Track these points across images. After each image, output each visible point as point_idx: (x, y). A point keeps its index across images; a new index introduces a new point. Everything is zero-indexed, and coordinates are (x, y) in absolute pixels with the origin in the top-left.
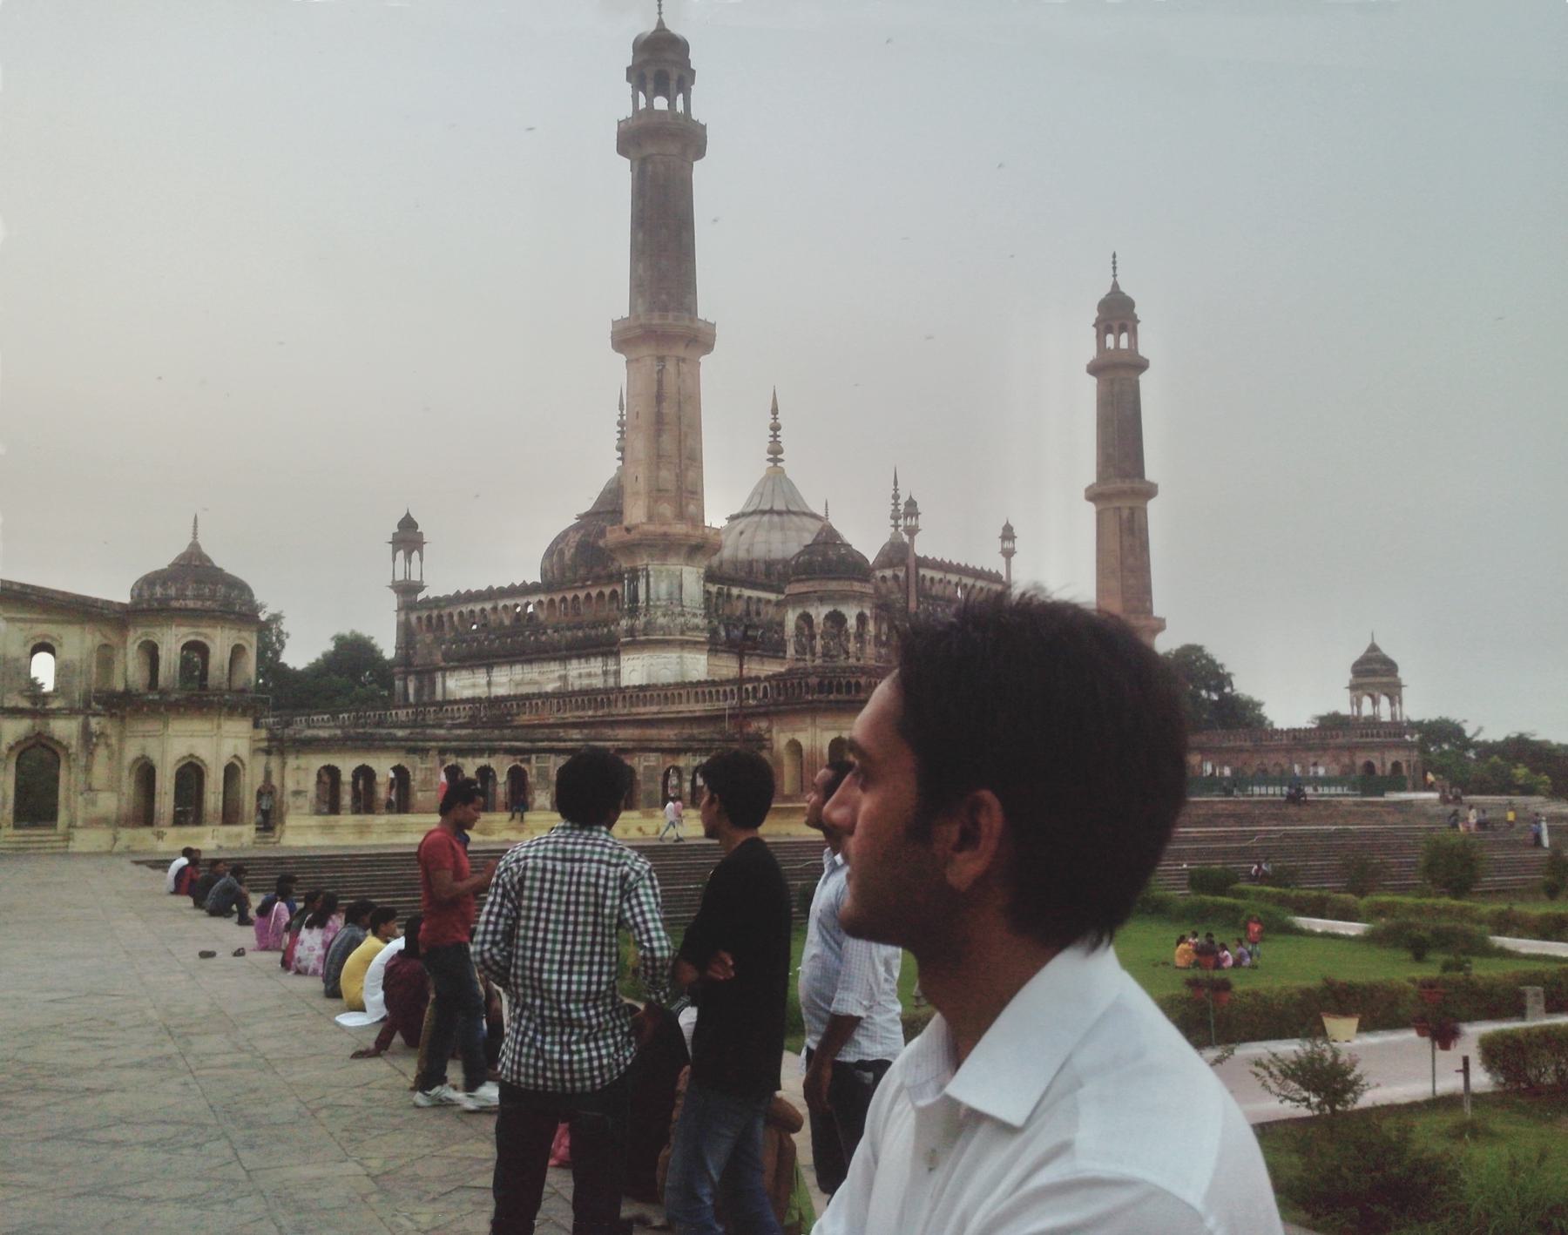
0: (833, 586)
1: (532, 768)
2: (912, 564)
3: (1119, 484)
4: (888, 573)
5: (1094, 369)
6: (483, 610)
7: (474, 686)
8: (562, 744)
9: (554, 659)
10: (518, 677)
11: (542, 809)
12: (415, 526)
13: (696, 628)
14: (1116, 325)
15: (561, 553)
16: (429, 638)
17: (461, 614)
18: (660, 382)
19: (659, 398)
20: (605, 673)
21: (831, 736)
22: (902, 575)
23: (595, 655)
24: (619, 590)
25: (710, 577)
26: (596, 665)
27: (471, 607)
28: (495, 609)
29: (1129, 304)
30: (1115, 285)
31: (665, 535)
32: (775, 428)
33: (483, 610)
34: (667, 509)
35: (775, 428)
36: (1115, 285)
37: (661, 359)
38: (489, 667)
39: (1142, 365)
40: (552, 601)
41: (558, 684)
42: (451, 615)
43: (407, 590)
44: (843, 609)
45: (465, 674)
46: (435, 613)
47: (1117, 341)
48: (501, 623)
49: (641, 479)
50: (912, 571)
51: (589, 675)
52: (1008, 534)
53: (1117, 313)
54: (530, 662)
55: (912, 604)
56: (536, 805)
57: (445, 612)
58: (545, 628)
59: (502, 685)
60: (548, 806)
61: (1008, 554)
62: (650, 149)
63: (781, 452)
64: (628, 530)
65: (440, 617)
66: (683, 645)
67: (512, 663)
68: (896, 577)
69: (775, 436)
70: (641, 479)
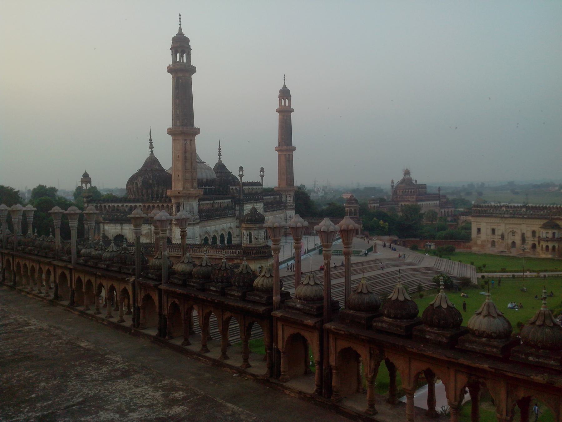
0: (258, 225)
2: (241, 185)
3: (285, 148)
4: (234, 188)
5: (278, 111)
6: (118, 206)
7: (116, 229)
12: (88, 175)
13: (197, 219)
15: (136, 184)
17: (109, 206)
19: (185, 152)
21: (259, 266)
22: (238, 189)
24: (170, 205)
27: (113, 204)
28: (123, 206)
29: (289, 91)
30: (285, 85)
31: (189, 194)
33: (118, 206)
34: (188, 185)
36: (285, 85)
37: (186, 140)
38: (122, 224)
39: (293, 111)
40: (144, 206)
42: (105, 206)
45: (112, 225)
46: (99, 205)
47: (285, 102)
48: (125, 210)
49: (180, 176)
50: (241, 189)
52: (262, 170)
53: (285, 94)
55: (242, 198)
57: (103, 205)
59: (126, 229)
61: (262, 176)
62: (180, 75)
64: (179, 193)
65: (101, 206)
66: (194, 224)
68: (236, 189)
70: (180, 176)
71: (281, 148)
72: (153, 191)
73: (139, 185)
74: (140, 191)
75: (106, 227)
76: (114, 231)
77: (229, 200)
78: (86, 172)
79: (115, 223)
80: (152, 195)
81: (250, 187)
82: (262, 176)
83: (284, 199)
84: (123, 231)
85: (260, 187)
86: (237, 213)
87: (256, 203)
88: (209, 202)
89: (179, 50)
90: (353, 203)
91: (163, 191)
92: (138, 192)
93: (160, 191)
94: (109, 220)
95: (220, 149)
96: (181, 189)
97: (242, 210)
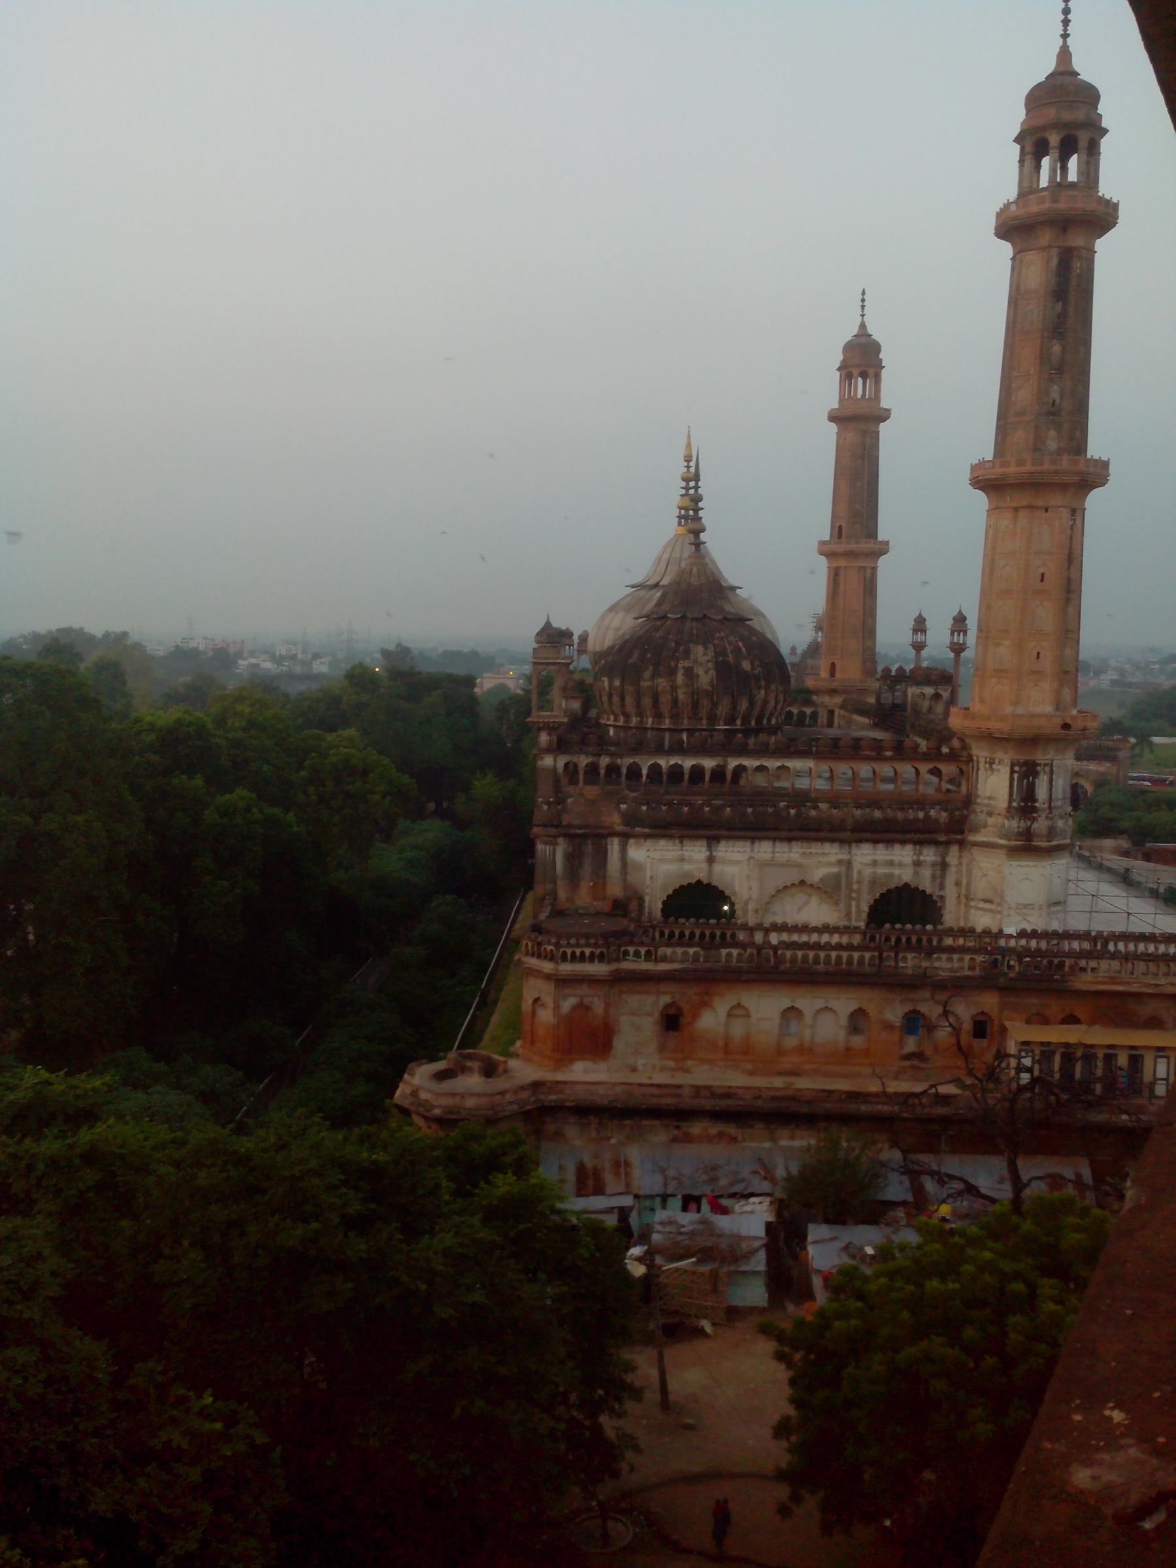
9: (833, 841)
10: (768, 856)
15: (690, 673)
16: (592, 791)
17: (655, 768)
20: (917, 864)
23: (903, 842)
26: (904, 854)
30: (863, 326)
36: (863, 326)
37: (1074, 512)
38: (712, 841)
41: (835, 870)
45: (662, 843)
46: (604, 761)
51: (891, 863)
53: (862, 359)
54: (790, 840)
57: (625, 762)
58: (815, 802)
61: (919, 647)
64: (1066, 726)
67: (753, 839)
71: (853, 546)
72: (752, 703)
73: (705, 677)
74: (705, 703)
75: (638, 852)
76: (673, 868)
78: (548, 625)
79: (682, 838)
80: (746, 720)
84: (717, 868)
89: (1054, 139)
91: (775, 707)
92: (695, 705)
93: (772, 704)
94: (654, 826)
96: (1048, 709)
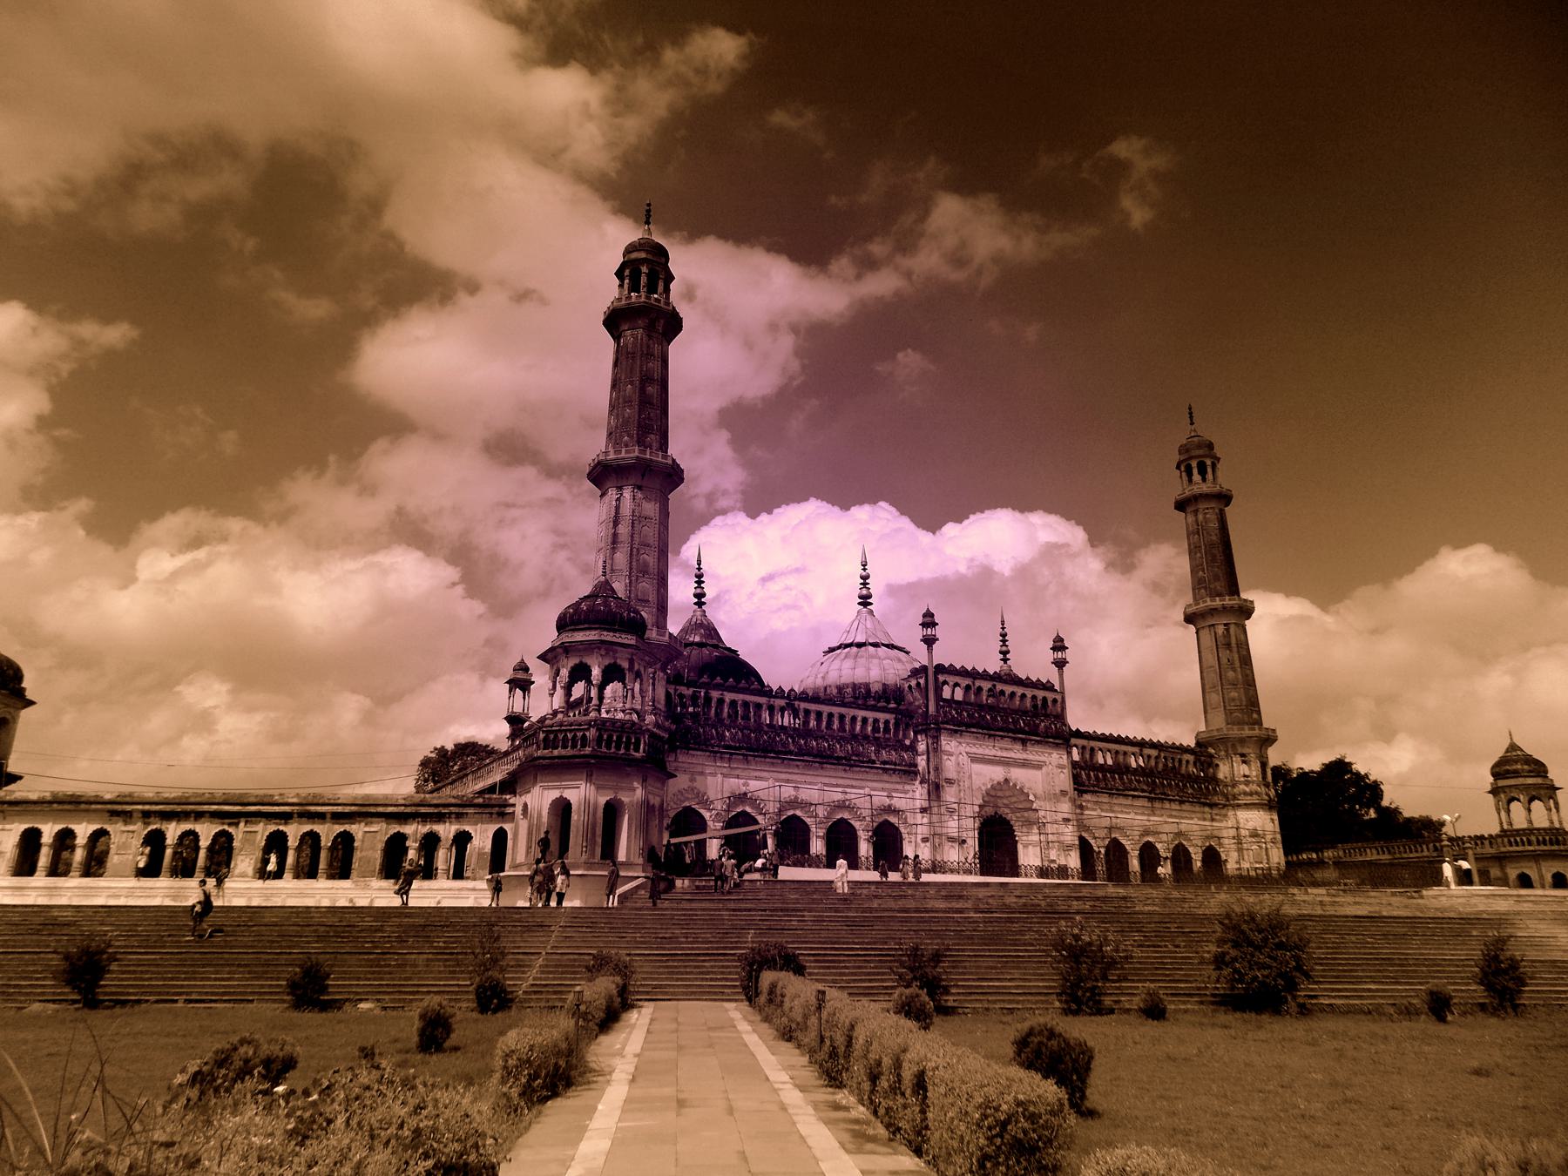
0: (580, 636)
1: (239, 832)
8: (276, 809)
11: (243, 875)
14: (1194, 464)
18: (617, 508)
19: (616, 523)
22: (922, 681)
25: (676, 679)
32: (865, 578)
35: (865, 578)
43: (515, 720)
44: (588, 660)
52: (1059, 645)
55: (932, 709)
56: (237, 872)
60: (250, 871)
61: (1060, 664)
63: (870, 596)
68: (918, 684)
69: (865, 584)
77: (882, 716)
81: (986, 685)
82: (1060, 664)
83: (1223, 771)
85: (1040, 694)
86: (921, 762)
87: (1024, 742)
88: (763, 700)
90: (1516, 774)
95: (1004, 635)
97: (935, 750)
